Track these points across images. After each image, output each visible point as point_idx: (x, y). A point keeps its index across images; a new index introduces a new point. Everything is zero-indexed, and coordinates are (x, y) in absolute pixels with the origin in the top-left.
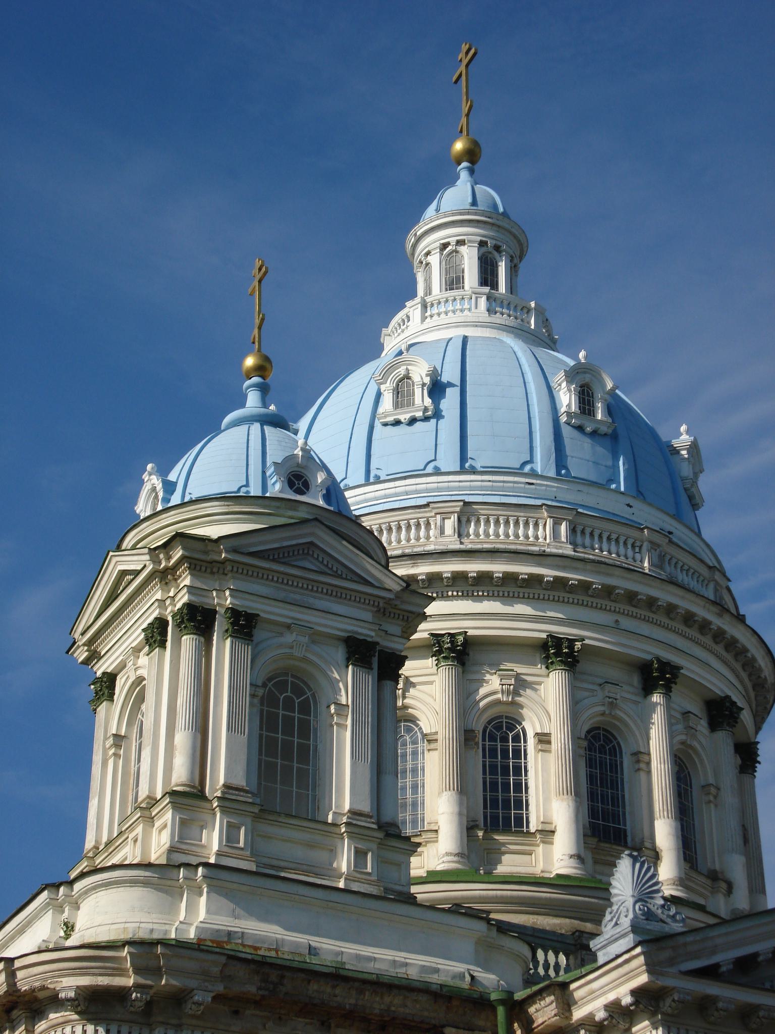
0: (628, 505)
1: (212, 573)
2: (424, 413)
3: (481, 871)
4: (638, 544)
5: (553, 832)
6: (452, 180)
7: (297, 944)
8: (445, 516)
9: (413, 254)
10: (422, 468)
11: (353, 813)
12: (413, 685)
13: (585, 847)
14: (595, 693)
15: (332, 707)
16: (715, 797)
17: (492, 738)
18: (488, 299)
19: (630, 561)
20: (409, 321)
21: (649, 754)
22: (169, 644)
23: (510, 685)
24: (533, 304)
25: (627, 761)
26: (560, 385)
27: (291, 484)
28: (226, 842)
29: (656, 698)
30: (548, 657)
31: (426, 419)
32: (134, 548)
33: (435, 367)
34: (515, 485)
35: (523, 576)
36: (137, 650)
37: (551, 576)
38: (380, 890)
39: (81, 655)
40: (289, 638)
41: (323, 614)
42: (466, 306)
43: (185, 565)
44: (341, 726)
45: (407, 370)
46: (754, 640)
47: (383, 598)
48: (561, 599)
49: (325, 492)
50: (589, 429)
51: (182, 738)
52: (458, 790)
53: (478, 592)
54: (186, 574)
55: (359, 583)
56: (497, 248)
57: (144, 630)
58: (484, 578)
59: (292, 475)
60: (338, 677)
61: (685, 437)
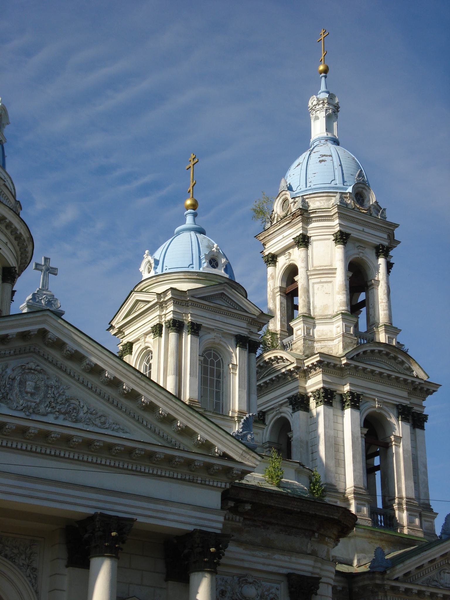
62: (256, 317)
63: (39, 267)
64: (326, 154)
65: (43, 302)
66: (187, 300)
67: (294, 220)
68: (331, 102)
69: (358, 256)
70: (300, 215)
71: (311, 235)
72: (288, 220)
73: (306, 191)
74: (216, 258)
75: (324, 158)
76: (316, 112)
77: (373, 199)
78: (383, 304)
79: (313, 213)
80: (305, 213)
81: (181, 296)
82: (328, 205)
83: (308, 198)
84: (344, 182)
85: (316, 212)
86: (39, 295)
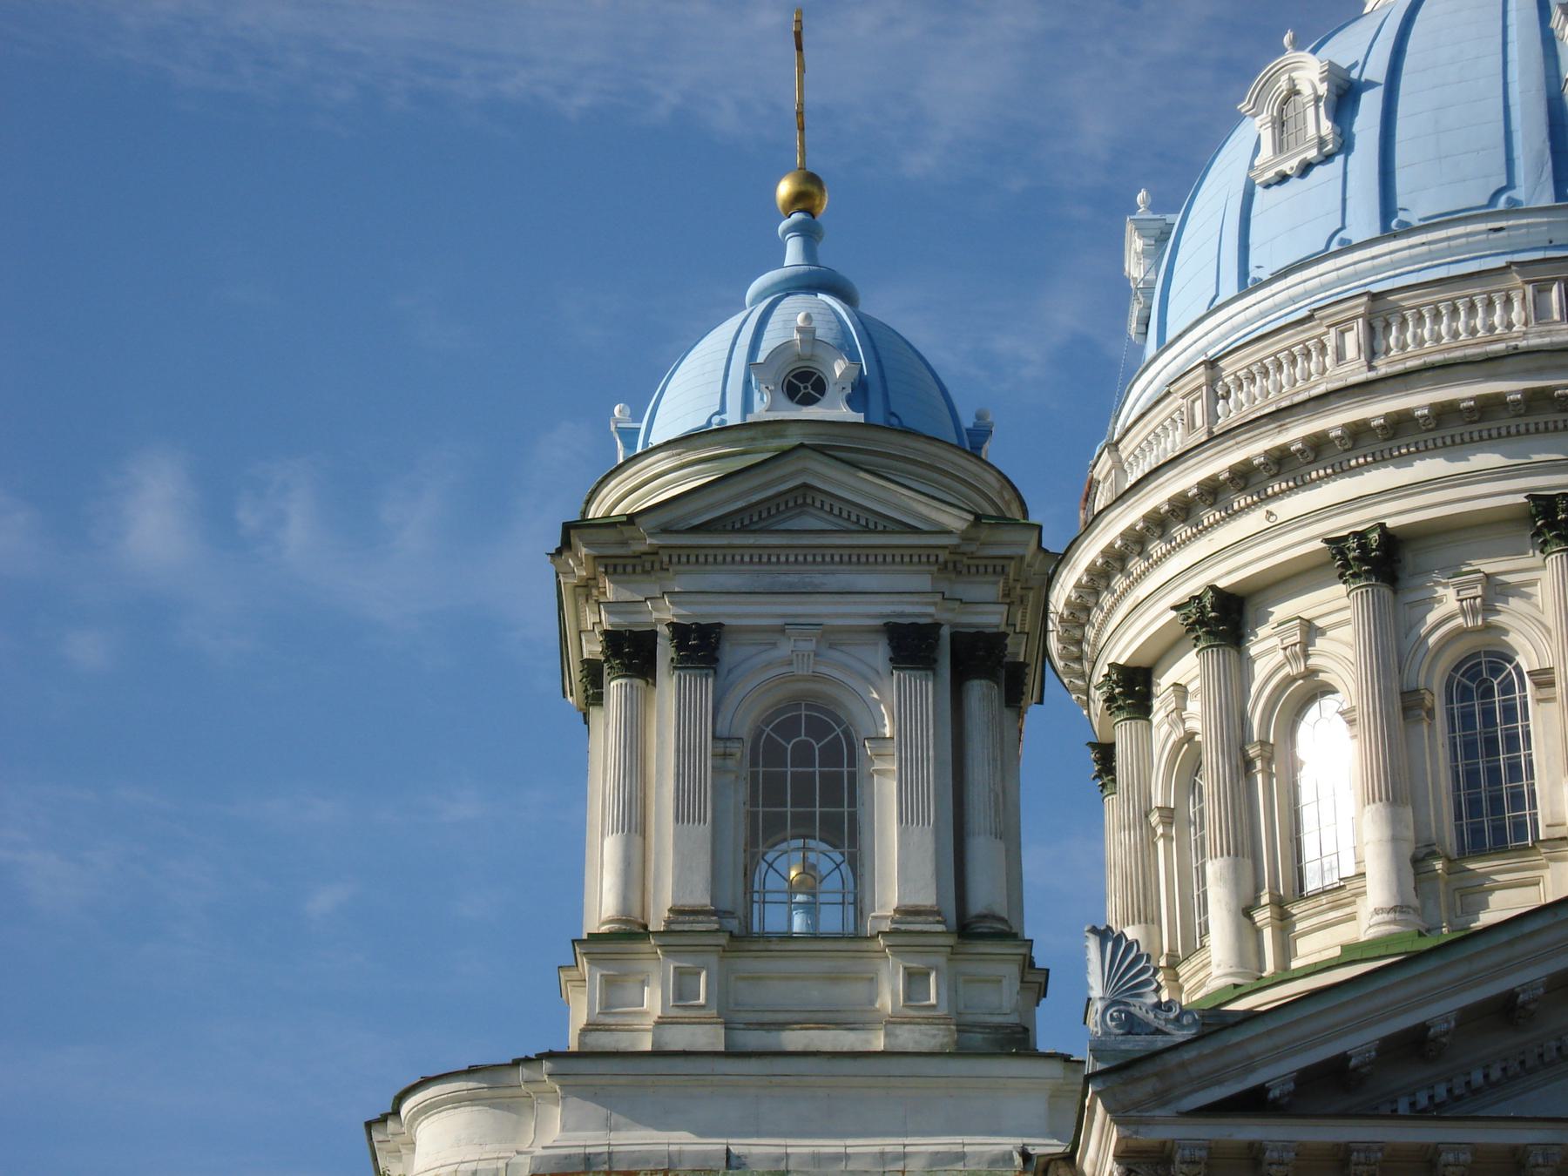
1: (645, 572)
2: (1320, 149)
3: (1444, 929)
7: (706, 1156)
8: (1342, 327)
12: (1321, 632)
17: (1465, 694)
23: (1475, 598)
28: (674, 1000)
30: (1538, 533)
31: (1327, 158)
33: (1331, 63)
34: (1471, 239)
35: (1465, 404)
37: (1516, 392)
38: (949, 1030)
40: (785, 648)
41: (837, 598)
45: (1291, 80)
47: (944, 547)
48: (1551, 426)
52: (1388, 799)
53: (1399, 448)
58: (1399, 425)
59: (793, 377)
60: (875, 696)
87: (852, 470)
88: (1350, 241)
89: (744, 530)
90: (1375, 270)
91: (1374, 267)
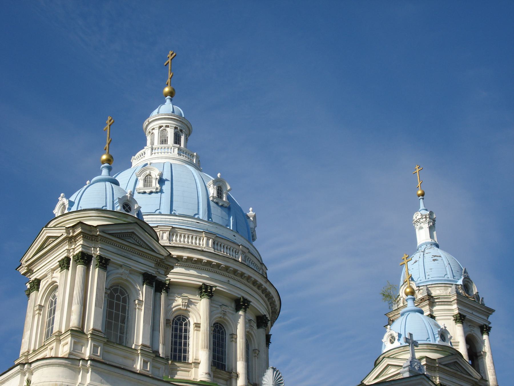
0: (234, 236)
1: (92, 240)
2: (156, 190)
4: (237, 251)
5: (199, 363)
6: (164, 102)
8: (164, 232)
9: (146, 129)
10: (154, 212)
11: (143, 345)
13: (211, 370)
14: (218, 309)
15: (137, 302)
16: (258, 355)
17: (176, 324)
18: (178, 149)
19: (234, 257)
20: (145, 154)
21: (237, 335)
22: (70, 268)
23: (186, 303)
24: (195, 154)
25: (228, 337)
26: (210, 185)
27: (124, 208)
29: (241, 313)
30: (201, 293)
31: (157, 192)
32: (54, 227)
34: (192, 223)
35: (195, 259)
36: (53, 270)
39: (23, 271)
40: (121, 271)
42: (169, 151)
43: (81, 236)
44: (140, 309)
46: (276, 294)
47: (159, 258)
48: (208, 270)
49: (137, 212)
50: (220, 204)
51: (76, 308)
52: (162, 343)
54: (81, 239)
55: (151, 251)
56: (181, 131)
57: (58, 261)
59: (125, 204)
60: (139, 289)
61: (251, 212)
62: (478, 381)
63: (408, 341)
64: (437, 255)
65: (416, 367)
66: (435, 366)
67: (422, 303)
68: (431, 217)
69: (470, 333)
70: (428, 300)
71: (436, 315)
72: (417, 303)
73: (427, 281)
74: (444, 334)
75: (436, 258)
76: (420, 223)
77: (475, 290)
78: (491, 370)
79: (437, 298)
80: (431, 299)
81: (431, 363)
82: (446, 293)
83: (430, 287)
84: (454, 276)
85: (439, 298)
86: (413, 362)
87: (145, 232)
88: (161, 213)
89: (119, 238)
90: (174, 222)
91: (170, 221)
